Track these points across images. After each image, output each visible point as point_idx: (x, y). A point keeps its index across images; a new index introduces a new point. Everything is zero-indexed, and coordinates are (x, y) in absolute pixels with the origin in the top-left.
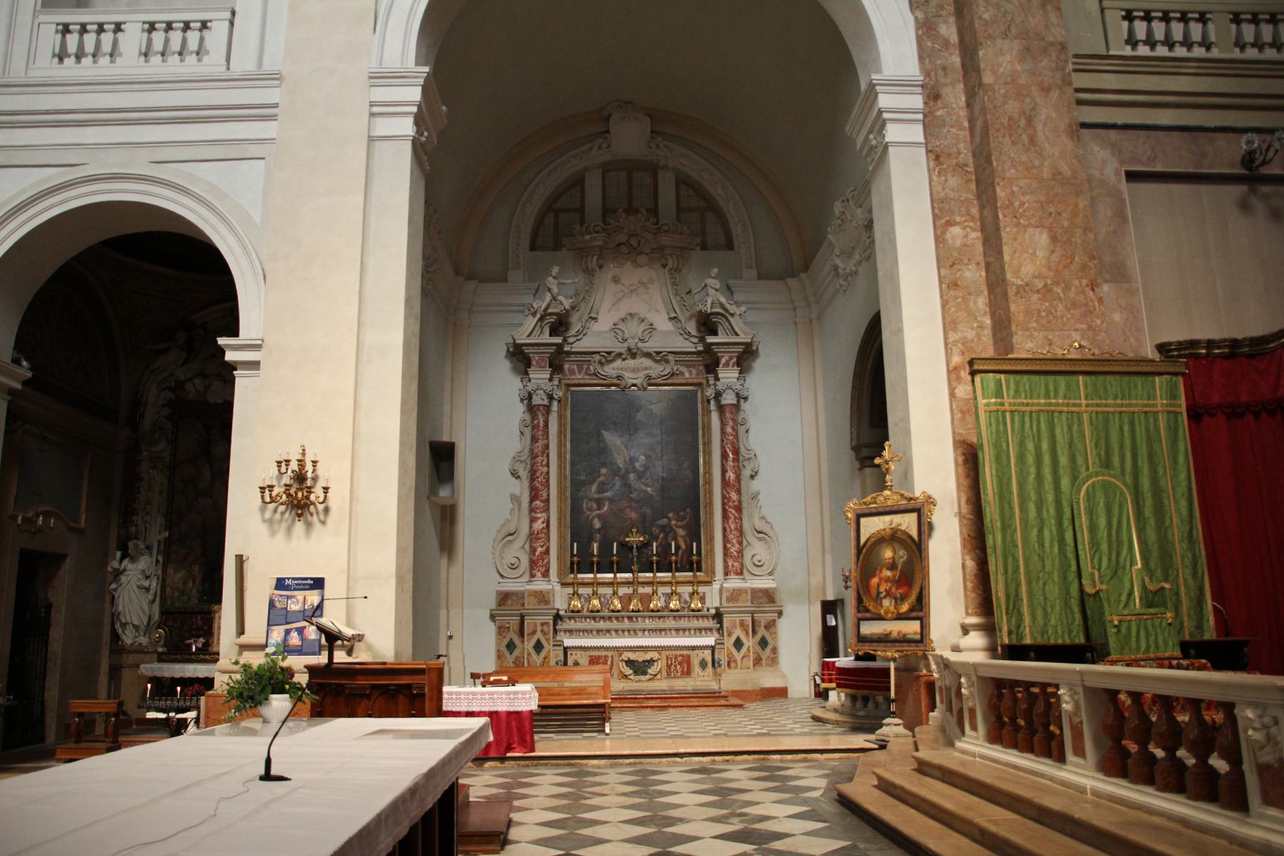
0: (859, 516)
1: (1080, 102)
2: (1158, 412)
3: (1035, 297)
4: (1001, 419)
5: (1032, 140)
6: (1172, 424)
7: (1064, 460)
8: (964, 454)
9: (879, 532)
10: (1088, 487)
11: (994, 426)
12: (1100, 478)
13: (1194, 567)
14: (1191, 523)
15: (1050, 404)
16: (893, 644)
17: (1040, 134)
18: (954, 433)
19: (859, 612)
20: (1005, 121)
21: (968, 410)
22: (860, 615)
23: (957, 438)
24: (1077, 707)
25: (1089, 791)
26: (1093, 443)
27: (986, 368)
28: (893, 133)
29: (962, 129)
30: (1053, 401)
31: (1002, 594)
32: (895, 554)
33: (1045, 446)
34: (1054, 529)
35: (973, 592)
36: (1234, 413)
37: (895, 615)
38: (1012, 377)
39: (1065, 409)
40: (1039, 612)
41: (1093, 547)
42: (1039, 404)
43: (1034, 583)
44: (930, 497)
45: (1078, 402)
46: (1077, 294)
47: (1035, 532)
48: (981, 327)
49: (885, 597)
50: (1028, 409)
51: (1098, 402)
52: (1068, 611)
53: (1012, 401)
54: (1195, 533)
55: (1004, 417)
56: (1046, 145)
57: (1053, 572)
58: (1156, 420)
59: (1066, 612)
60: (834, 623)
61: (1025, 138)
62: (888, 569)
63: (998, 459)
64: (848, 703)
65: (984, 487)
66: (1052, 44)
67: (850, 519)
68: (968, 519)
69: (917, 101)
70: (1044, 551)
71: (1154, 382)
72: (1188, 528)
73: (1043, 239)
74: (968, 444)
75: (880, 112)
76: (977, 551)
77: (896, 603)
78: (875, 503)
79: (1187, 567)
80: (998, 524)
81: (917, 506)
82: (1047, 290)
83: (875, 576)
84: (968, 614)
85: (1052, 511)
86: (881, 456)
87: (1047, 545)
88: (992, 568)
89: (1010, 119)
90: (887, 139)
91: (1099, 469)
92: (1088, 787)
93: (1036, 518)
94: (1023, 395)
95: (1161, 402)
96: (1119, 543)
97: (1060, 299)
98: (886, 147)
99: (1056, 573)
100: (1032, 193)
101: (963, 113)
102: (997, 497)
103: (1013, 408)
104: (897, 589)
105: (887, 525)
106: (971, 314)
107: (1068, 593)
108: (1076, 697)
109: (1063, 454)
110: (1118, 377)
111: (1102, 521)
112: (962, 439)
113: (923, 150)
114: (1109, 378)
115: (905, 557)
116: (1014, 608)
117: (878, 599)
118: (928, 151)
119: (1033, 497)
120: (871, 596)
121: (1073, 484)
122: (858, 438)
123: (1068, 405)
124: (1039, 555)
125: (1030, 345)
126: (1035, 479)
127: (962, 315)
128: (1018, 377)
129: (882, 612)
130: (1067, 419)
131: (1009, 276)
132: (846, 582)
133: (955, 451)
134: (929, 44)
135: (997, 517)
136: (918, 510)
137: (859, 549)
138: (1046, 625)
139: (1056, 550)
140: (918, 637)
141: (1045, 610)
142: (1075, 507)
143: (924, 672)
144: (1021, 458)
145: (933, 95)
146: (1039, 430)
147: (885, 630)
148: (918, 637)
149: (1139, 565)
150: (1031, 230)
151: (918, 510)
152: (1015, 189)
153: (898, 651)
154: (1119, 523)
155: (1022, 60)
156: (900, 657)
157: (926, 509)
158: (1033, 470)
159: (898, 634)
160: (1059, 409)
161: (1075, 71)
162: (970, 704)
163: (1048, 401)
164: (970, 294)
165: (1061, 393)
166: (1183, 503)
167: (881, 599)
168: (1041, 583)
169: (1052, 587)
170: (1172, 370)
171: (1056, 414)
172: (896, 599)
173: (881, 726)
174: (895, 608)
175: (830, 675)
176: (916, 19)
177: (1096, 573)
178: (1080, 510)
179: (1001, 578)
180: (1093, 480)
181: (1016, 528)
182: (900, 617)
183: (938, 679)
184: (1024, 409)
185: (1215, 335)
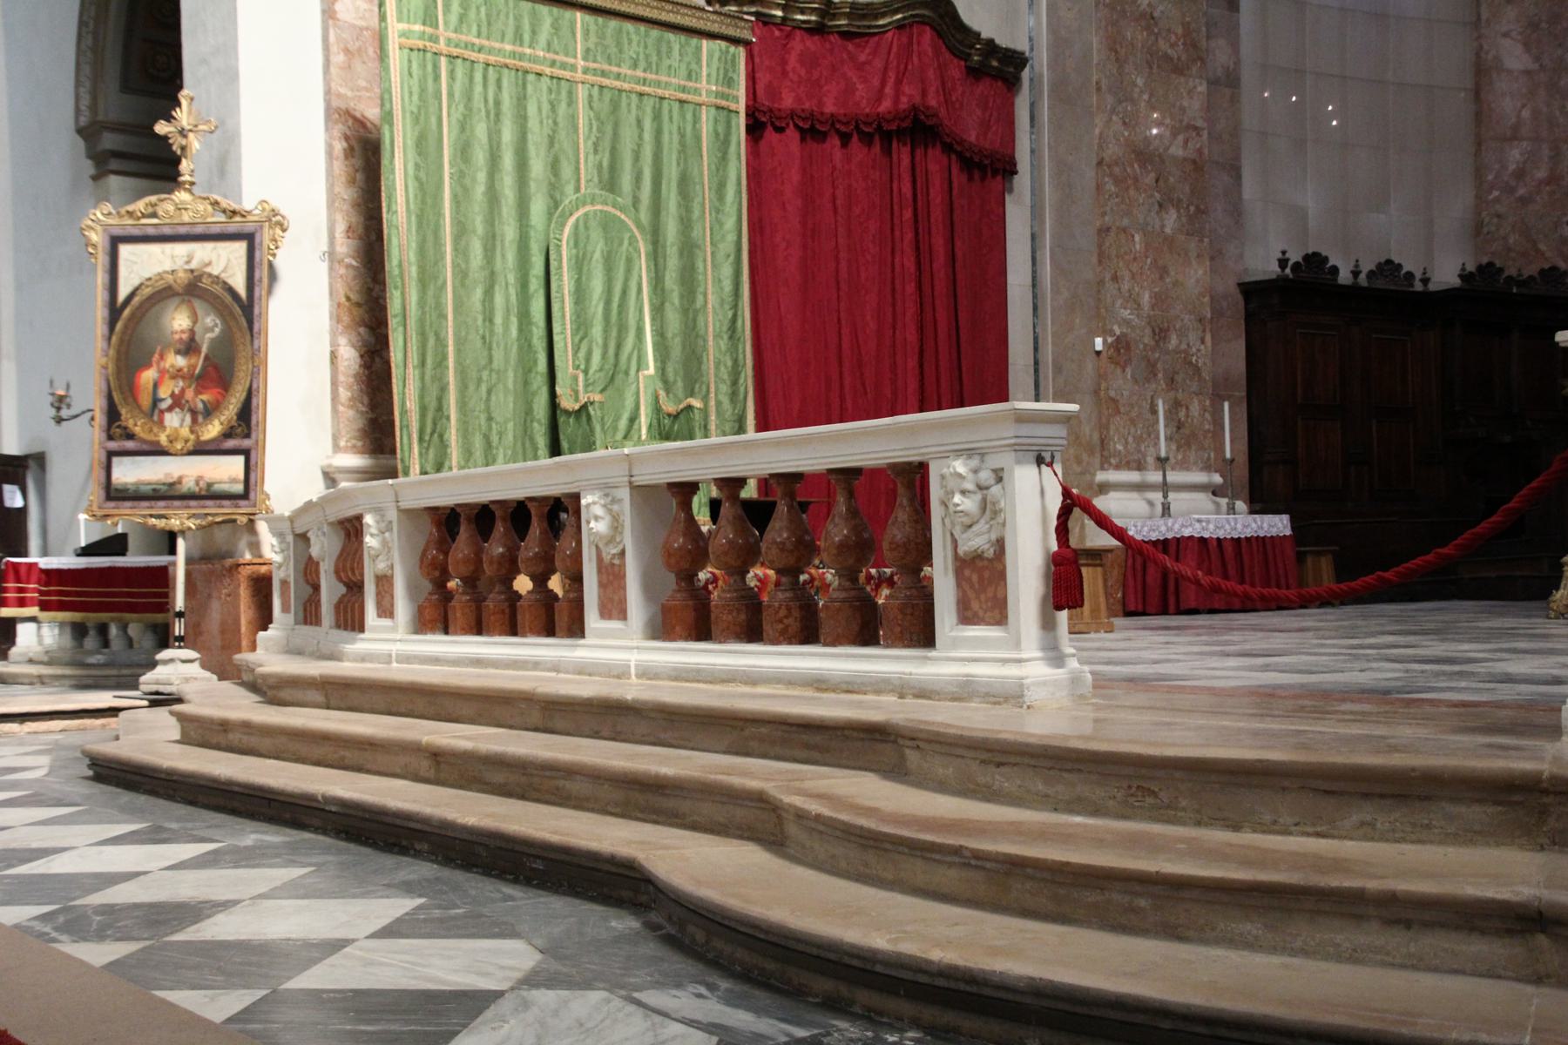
0: (116, 241)
2: (700, 105)
4: (430, 68)
6: (721, 129)
7: (537, 167)
8: (347, 138)
9: (160, 276)
10: (577, 220)
11: (415, 82)
12: (599, 207)
13: (735, 383)
14: (735, 307)
15: (521, 57)
16: (185, 503)
18: (328, 92)
19: (110, 438)
21: (359, 50)
22: (113, 445)
23: (335, 103)
24: (616, 526)
25: (633, 671)
26: (590, 143)
30: (528, 51)
31: (412, 405)
32: (195, 322)
33: (508, 135)
34: (512, 291)
35: (351, 407)
36: (813, 130)
37: (190, 446)
39: (548, 71)
41: (578, 329)
43: (472, 387)
44: (275, 213)
45: (571, 60)
47: (478, 293)
49: (170, 409)
50: (482, 57)
51: (606, 67)
52: (528, 444)
53: (453, 36)
54: (739, 323)
55: (436, 67)
57: (506, 370)
58: (696, 120)
59: (523, 444)
60: (18, 502)
62: (178, 352)
63: (421, 143)
64: (67, 641)
65: (389, 197)
67: (94, 246)
68: (348, 266)
70: (492, 332)
71: (699, 49)
72: (730, 314)
74: (355, 119)
76: (362, 330)
77: (194, 421)
78: (154, 215)
79: (724, 381)
80: (414, 269)
81: (249, 228)
83: (148, 365)
84: (337, 448)
85: (511, 257)
86: (169, 118)
87: (498, 320)
88: (396, 355)
91: (597, 191)
92: (632, 664)
93: (482, 268)
94: (474, 29)
95: (706, 88)
96: (622, 329)
99: (511, 374)
102: (413, 218)
103: (455, 51)
104: (198, 392)
105: (179, 264)
107: (529, 411)
108: (616, 507)
109: (537, 155)
110: (642, 28)
111: (597, 286)
112: (343, 106)
114: (629, 26)
115: (217, 330)
116: (433, 432)
117: (154, 411)
120: (139, 407)
121: (550, 214)
122: (93, 108)
123: (553, 64)
124: (483, 337)
126: (485, 194)
129: (163, 439)
130: (550, 91)
132: (59, 409)
133: (327, 129)
135: (412, 257)
136: (249, 238)
137: (115, 311)
139: (514, 332)
140: (239, 488)
141: (487, 438)
142: (553, 257)
143: (248, 557)
144: (464, 151)
146: (498, 103)
147: (167, 475)
148: (239, 488)
149: (651, 370)
151: (249, 238)
153: (194, 516)
154: (624, 292)
156: (200, 528)
157: (265, 237)
158: (482, 176)
159: (197, 483)
160: (538, 68)
162: (381, 566)
163: (519, 49)
165: (543, 38)
166: (727, 271)
167: (162, 412)
168: (484, 388)
169: (501, 396)
170: (731, 32)
171: (531, 77)
172: (194, 413)
173: (153, 665)
174: (192, 432)
175: (21, 590)
177: (581, 377)
178: (560, 261)
179: (413, 374)
180: (588, 208)
181: (445, 283)
182: (201, 450)
183: (280, 566)
184: (474, 56)
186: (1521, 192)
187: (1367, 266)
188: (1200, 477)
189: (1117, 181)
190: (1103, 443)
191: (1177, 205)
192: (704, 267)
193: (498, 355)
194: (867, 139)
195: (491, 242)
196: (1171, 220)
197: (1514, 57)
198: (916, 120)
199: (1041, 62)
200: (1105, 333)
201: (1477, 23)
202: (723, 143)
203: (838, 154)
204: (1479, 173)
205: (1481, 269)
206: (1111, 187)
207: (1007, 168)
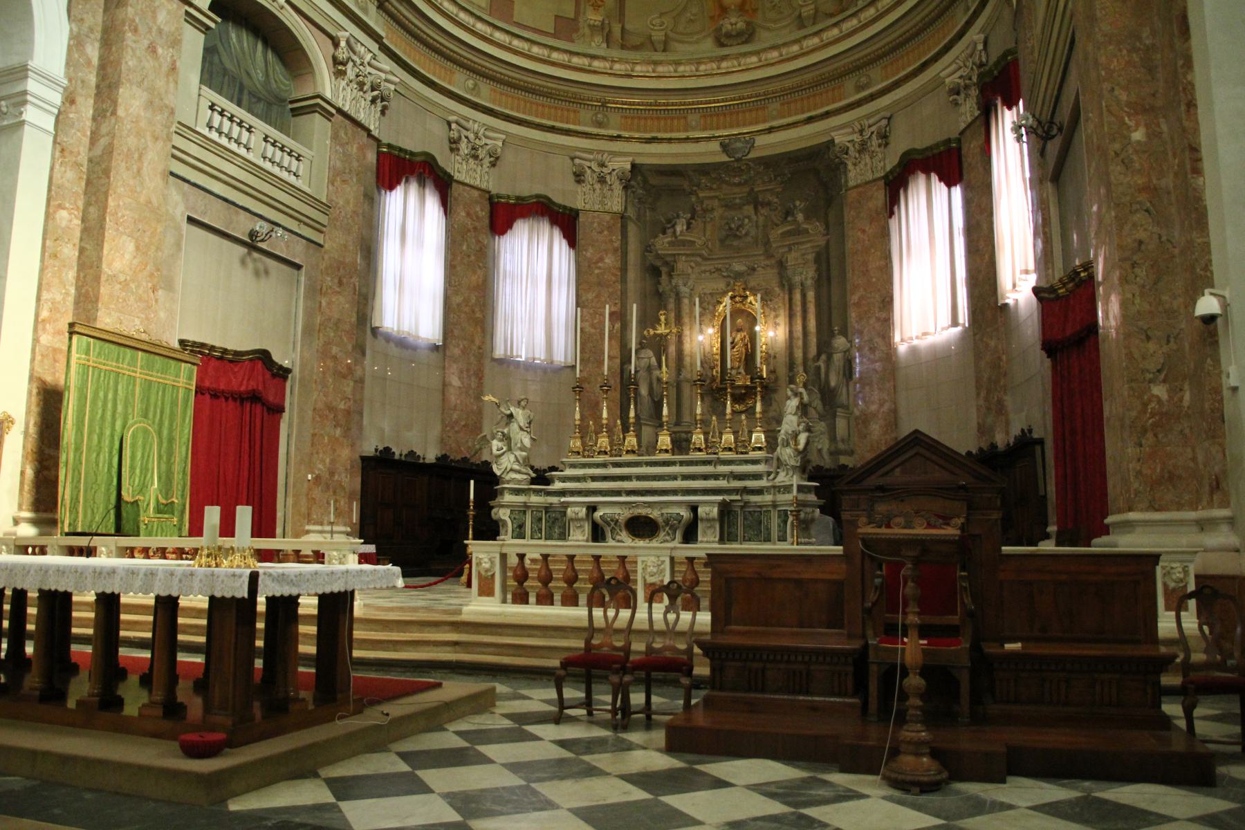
1: (174, 156)
3: (118, 287)
5: (139, 171)
13: (183, 491)
14: (185, 462)
15: (118, 367)
17: (145, 168)
18: (32, 370)
20: (125, 150)
27: (83, 331)
28: (30, 114)
29: (84, 135)
31: (67, 497)
33: (110, 396)
36: (215, 395)
38: (98, 342)
40: (89, 512)
42: (111, 366)
44: (9, 417)
46: (144, 292)
47: (94, 455)
48: (67, 294)
50: (104, 367)
56: (147, 178)
58: (178, 392)
61: (135, 167)
66: (167, 107)
69: (57, 98)
73: (131, 247)
75: (25, 93)
82: (125, 285)
84: (20, 508)
85: (107, 442)
87: (101, 465)
89: (129, 150)
90: (24, 117)
95: (182, 381)
96: (147, 470)
97: (132, 293)
98: (23, 123)
100: (131, 210)
101: (89, 123)
106: (63, 283)
107: (109, 500)
110: (162, 358)
111: (139, 455)
113: (51, 139)
114: (157, 358)
118: (55, 142)
119: (97, 431)
125: (108, 320)
127: (56, 281)
128: (102, 343)
131: (104, 266)
134: (76, 56)
138: (92, 521)
141: (93, 510)
145: (70, 99)
146: (108, 383)
150: (124, 237)
152: (121, 203)
155: (146, 109)
158: (100, 412)
161: (176, 132)
164: (64, 266)
165: (126, 361)
166: (184, 449)
176: (71, 30)
185: (217, 344)
186: (456, 429)
187: (405, 452)
188: (342, 529)
189: (320, 417)
190: (309, 515)
191: (341, 426)
192: (176, 447)
193: (99, 478)
194: (235, 400)
195: (101, 435)
196: (338, 432)
197: (455, 381)
198: (254, 395)
199: (296, 371)
200: (312, 473)
201: (444, 368)
202: (186, 401)
203: (224, 405)
204: (443, 420)
205: (442, 456)
206: (318, 419)
207: (281, 410)
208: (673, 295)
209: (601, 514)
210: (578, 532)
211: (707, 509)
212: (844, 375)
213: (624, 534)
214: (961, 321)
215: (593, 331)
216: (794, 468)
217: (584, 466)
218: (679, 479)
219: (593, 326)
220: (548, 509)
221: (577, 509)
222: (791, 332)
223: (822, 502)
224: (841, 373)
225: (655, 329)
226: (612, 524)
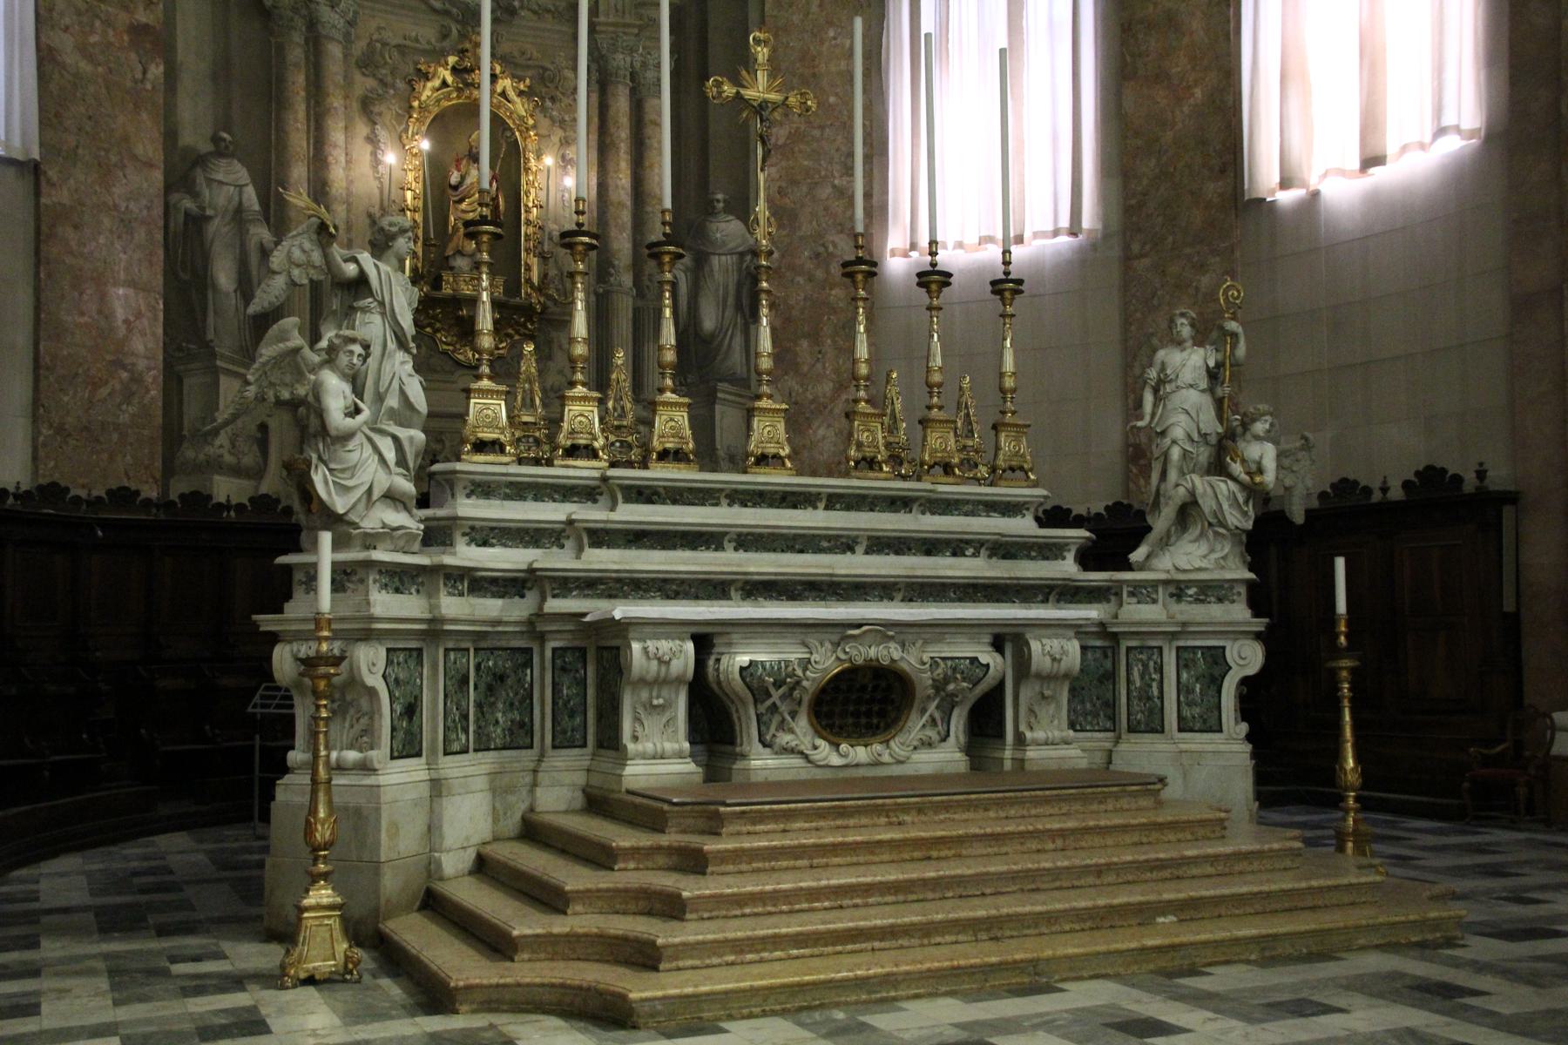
208: (300, 23)
209: (743, 659)
210: (652, 724)
211: (1054, 645)
212: (739, 307)
213: (801, 732)
214: (1087, 223)
215: (85, 66)
216: (1235, 533)
217: (519, 491)
218: (860, 549)
219: (83, 50)
220: (482, 639)
221: (665, 646)
222: (602, 187)
223: (1260, 624)
224: (731, 300)
225: (737, 81)
226: (776, 695)
